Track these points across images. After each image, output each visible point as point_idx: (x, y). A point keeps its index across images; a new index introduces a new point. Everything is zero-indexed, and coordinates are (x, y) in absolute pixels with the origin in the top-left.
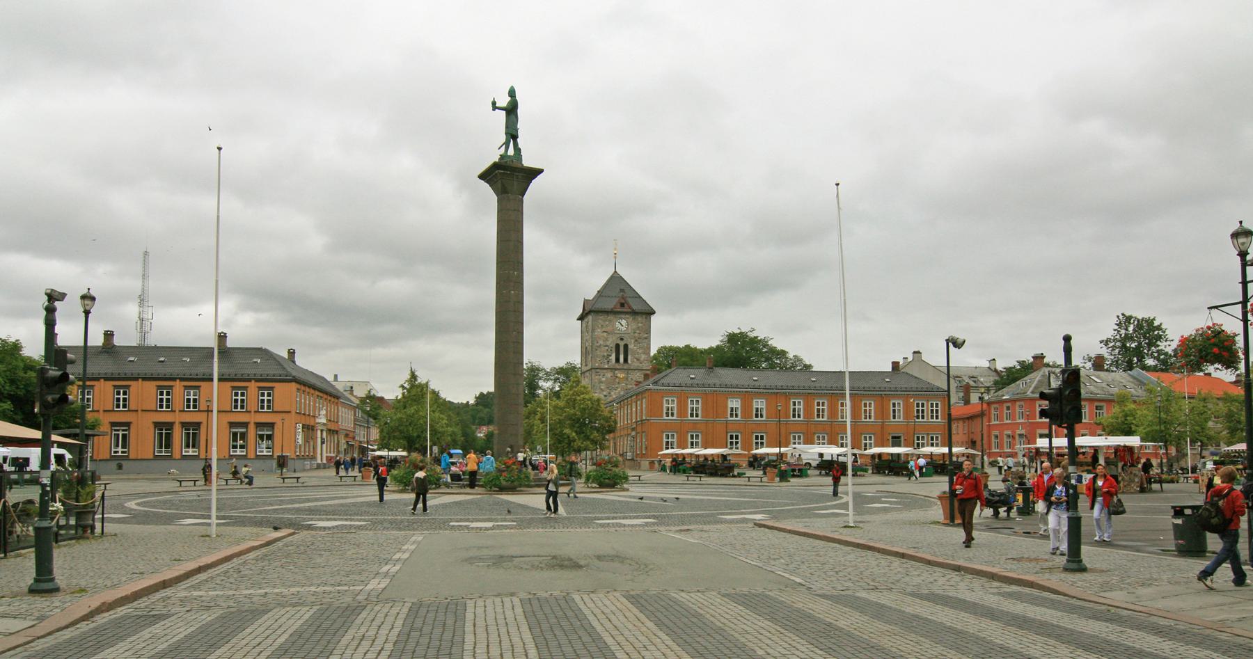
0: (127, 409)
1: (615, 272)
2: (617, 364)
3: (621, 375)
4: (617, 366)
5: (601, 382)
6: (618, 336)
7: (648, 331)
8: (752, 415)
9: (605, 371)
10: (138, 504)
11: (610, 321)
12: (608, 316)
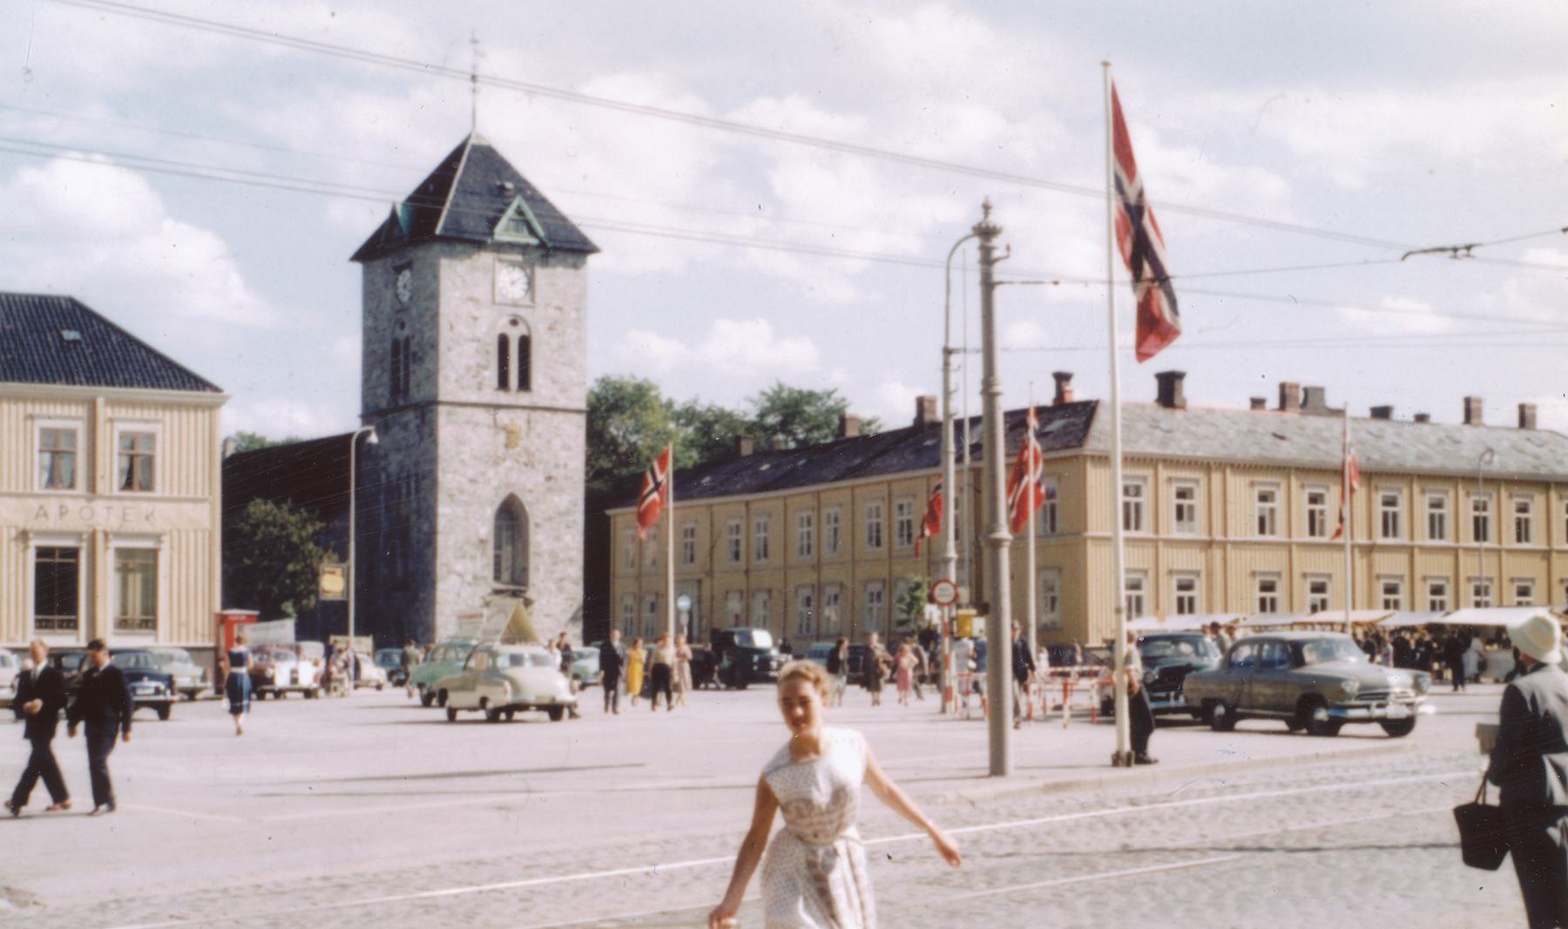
4: (503, 398)
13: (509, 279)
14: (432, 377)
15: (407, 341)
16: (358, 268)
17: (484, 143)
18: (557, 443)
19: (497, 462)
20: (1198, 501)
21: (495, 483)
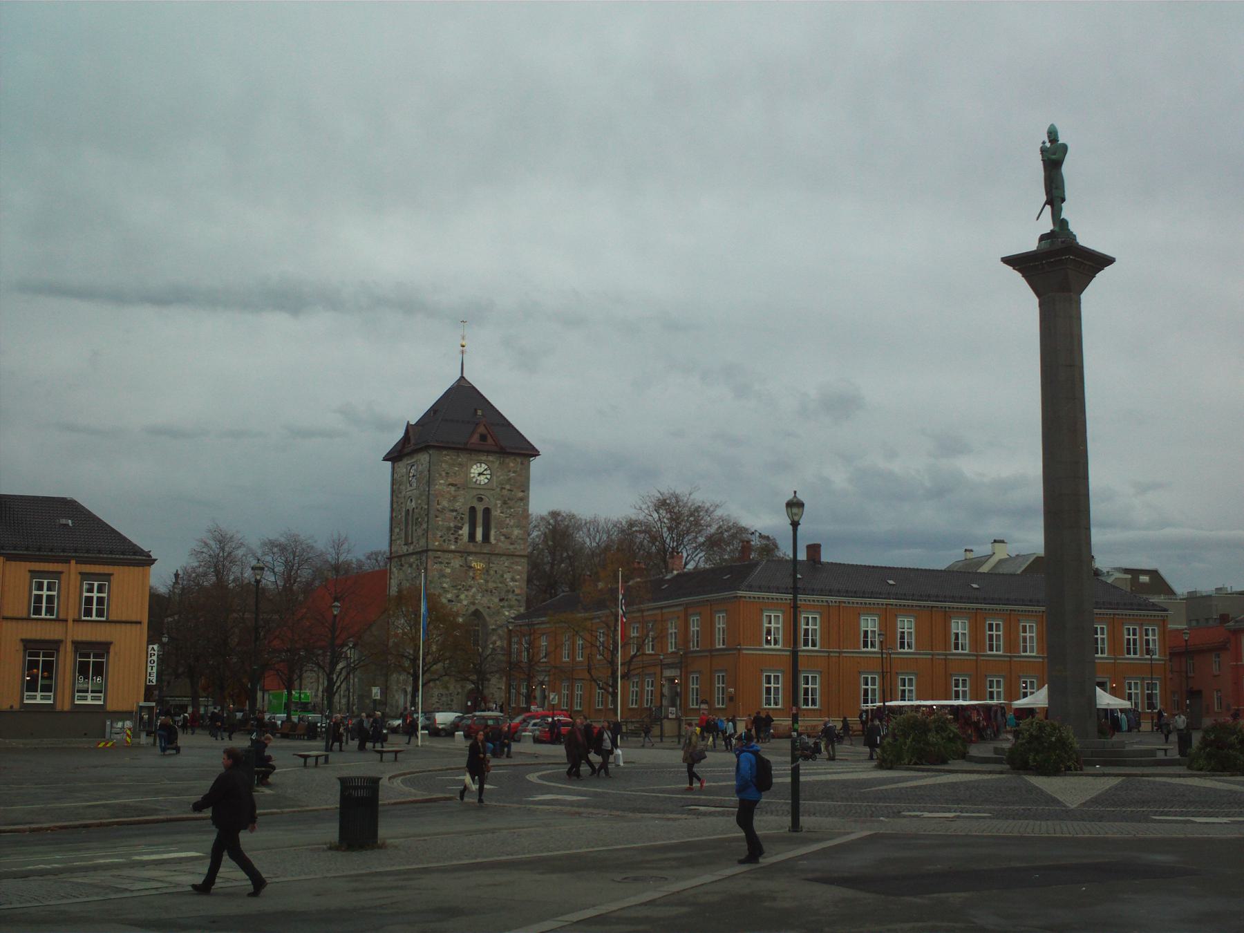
0: (104, 619)
1: (462, 377)
2: (471, 544)
3: (478, 565)
4: (471, 548)
5: (444, 576)
6: (475, 492)
7: (523, 486)
8: (950, 646)
9: (451, 555)
10: (540, 777)
11: (460, 465)
12: (458, 456)
13: (478, 472)
18: (507, 576)
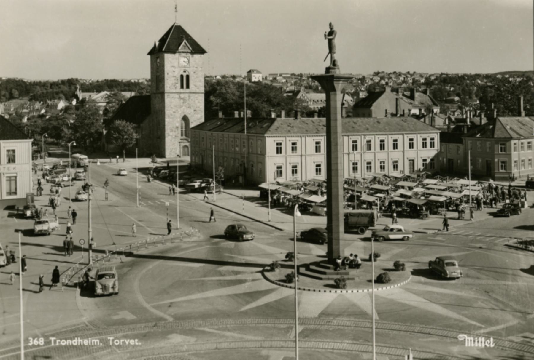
4: (182, 91)
14: (164, 86)
15: (159, 76)
16: (149, 57)
17: (178, 25)
18: (197, 101)
19: (181, 107)
20: (298, 146)
21: (180, 112)
